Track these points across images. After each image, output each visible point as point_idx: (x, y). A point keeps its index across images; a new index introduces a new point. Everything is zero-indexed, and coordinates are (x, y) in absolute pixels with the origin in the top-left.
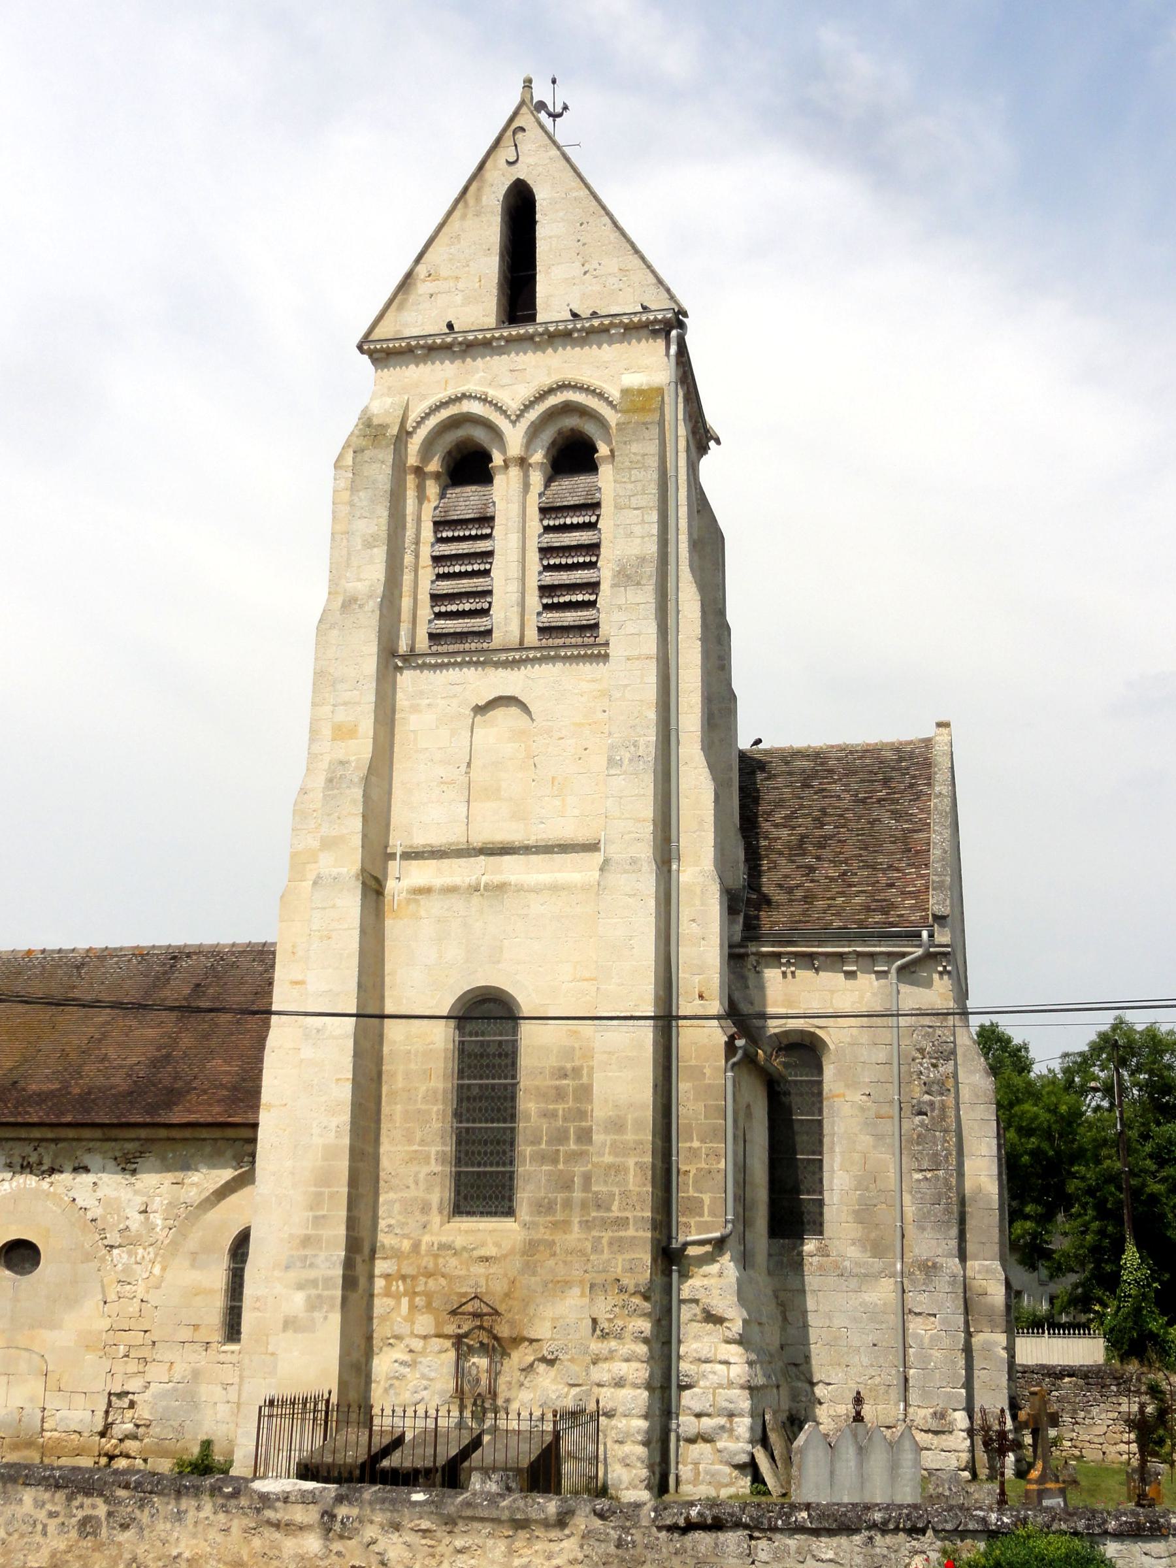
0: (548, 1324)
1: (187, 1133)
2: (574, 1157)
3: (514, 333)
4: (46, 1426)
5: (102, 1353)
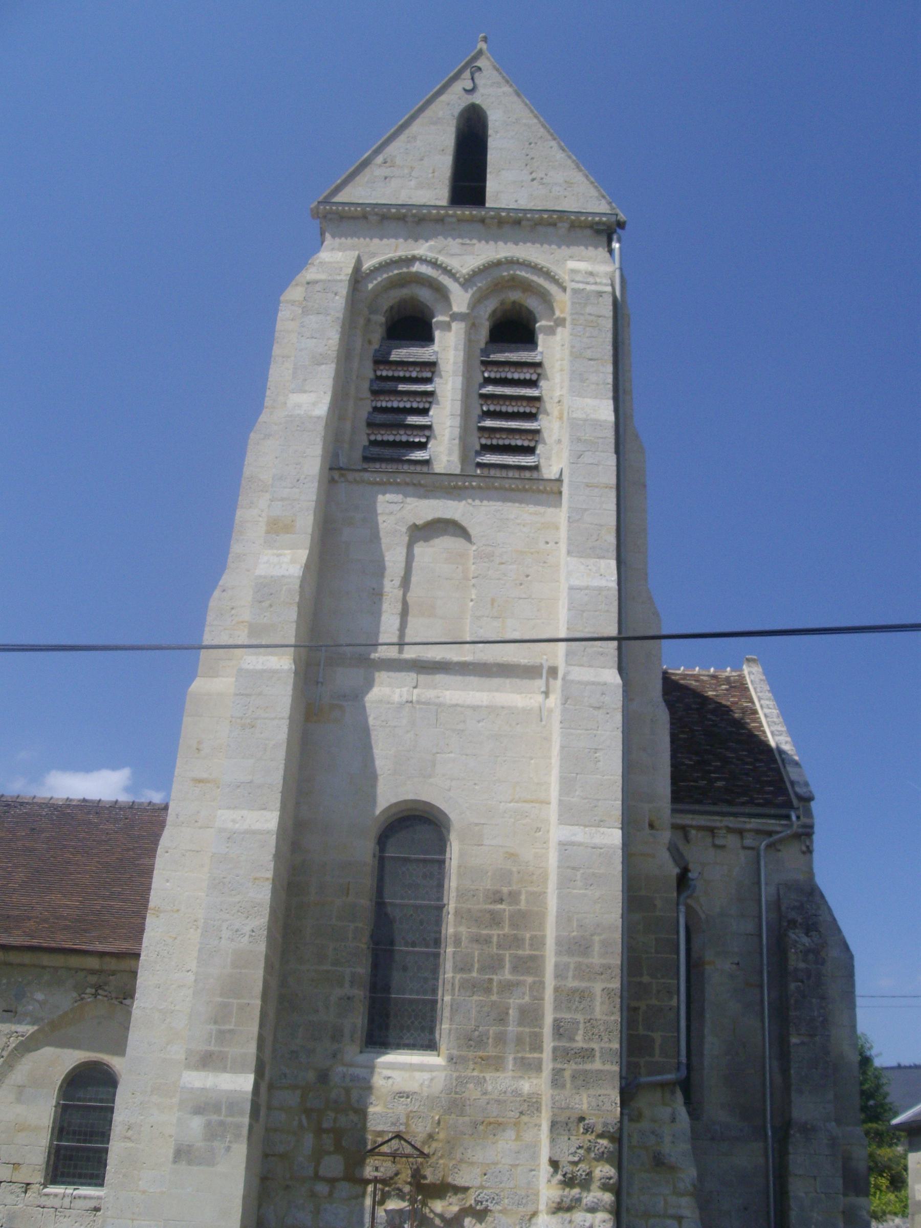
0: (478, 1171)
1: (27, 958)
2: (508, 987)
3: (467, 213)
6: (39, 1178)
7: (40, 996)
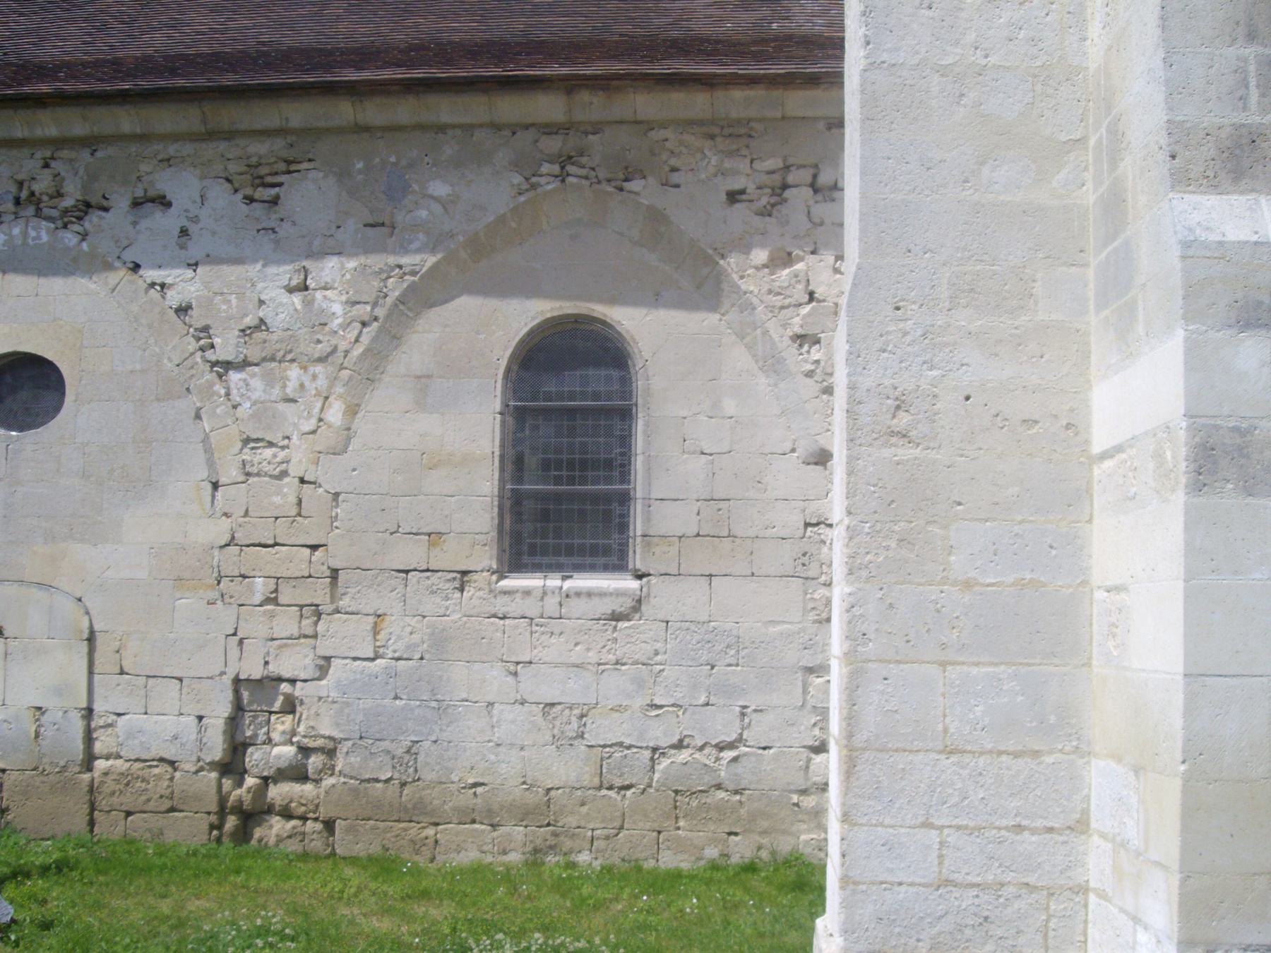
4: (98, 747)
5: (216, 595)
6: (485, 558)
7: (440, 189)
